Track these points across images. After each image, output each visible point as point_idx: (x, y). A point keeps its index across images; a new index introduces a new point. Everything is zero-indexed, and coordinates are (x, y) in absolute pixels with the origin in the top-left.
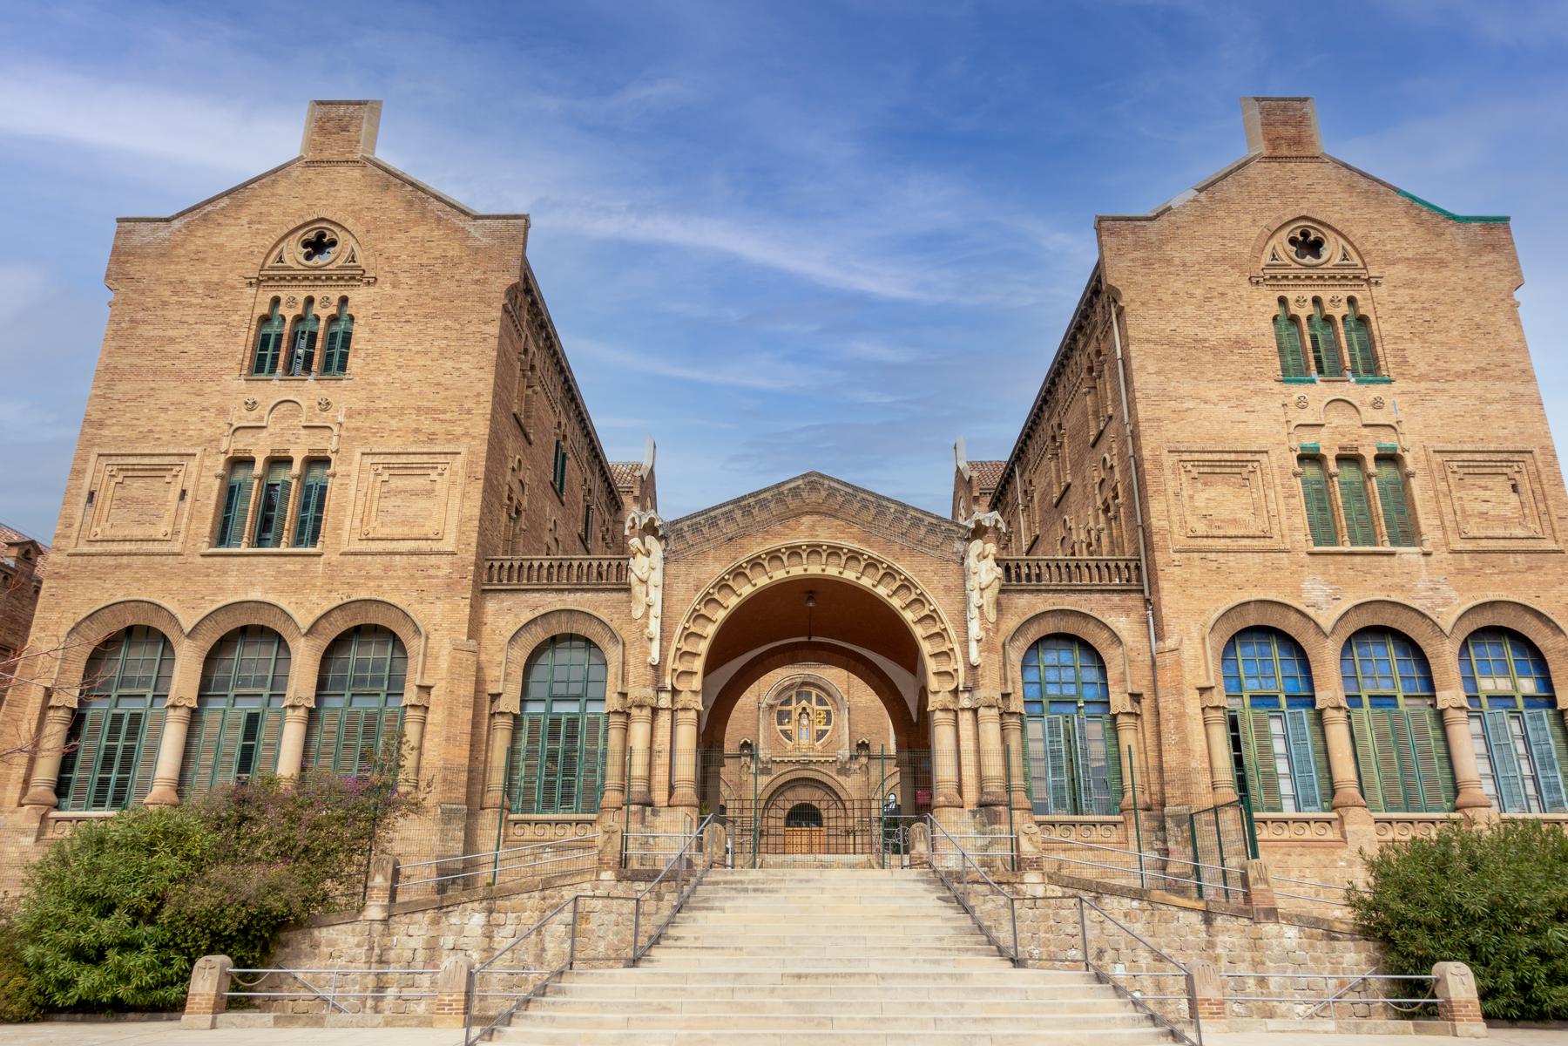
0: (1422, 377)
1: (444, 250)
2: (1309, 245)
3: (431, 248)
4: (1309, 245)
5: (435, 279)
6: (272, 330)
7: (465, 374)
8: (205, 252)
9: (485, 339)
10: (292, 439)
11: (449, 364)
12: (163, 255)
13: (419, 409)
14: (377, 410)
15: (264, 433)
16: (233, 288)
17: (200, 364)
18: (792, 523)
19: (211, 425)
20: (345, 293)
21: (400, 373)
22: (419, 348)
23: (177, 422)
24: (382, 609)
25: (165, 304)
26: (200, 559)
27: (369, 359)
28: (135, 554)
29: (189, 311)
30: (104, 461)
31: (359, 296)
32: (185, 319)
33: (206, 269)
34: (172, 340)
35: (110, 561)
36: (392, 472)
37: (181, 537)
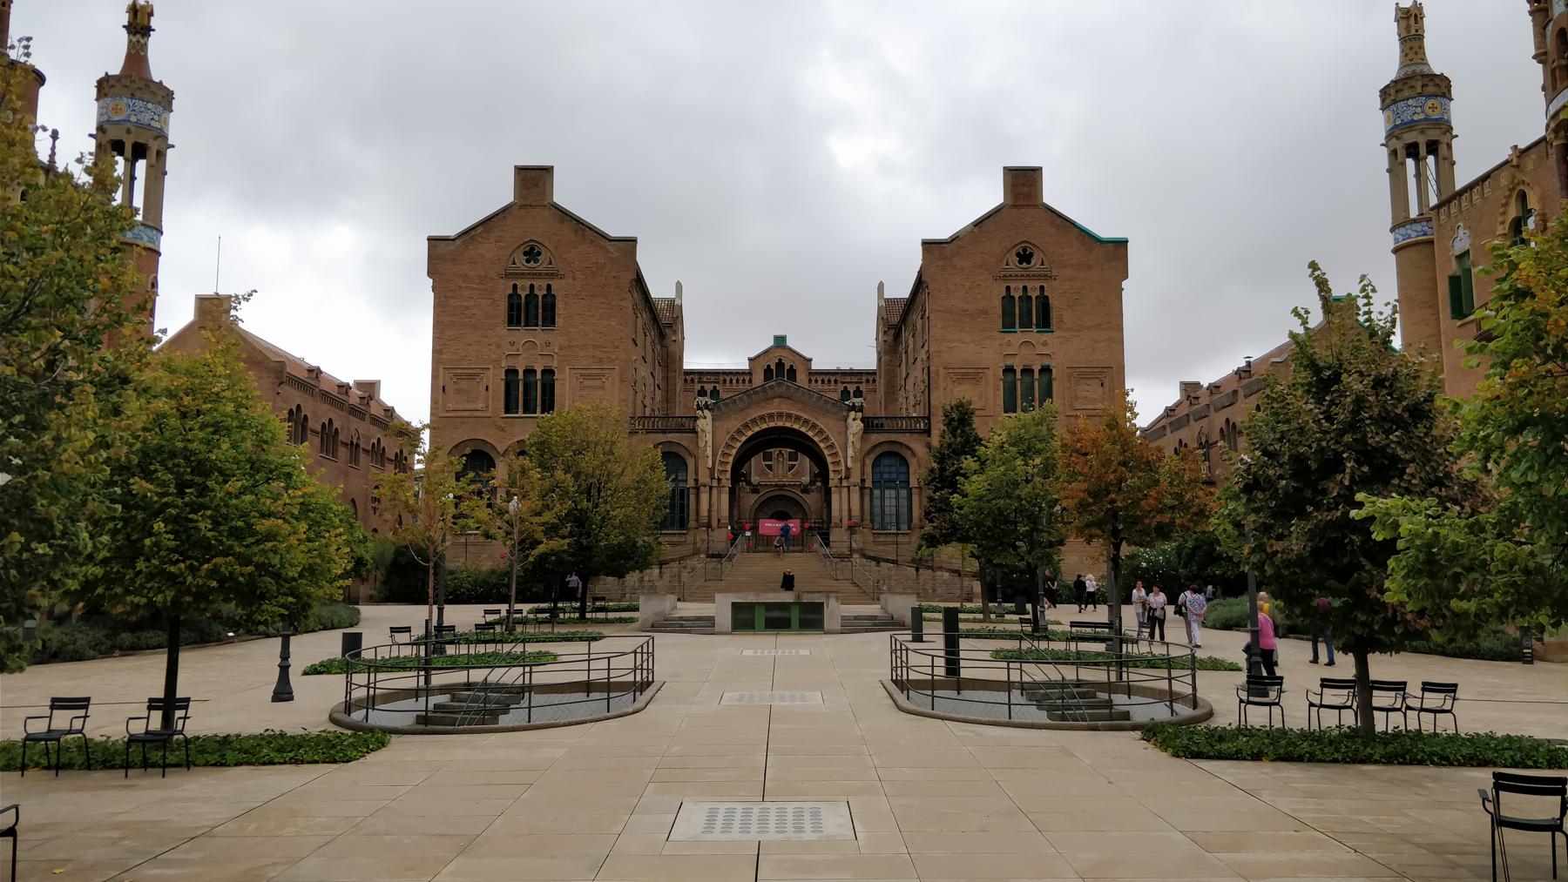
0: (1069, 329)
2: (1025, 257)
4: (1025, 257)
6: (515, 301)
11: (606, 322)
34: (467, 307)
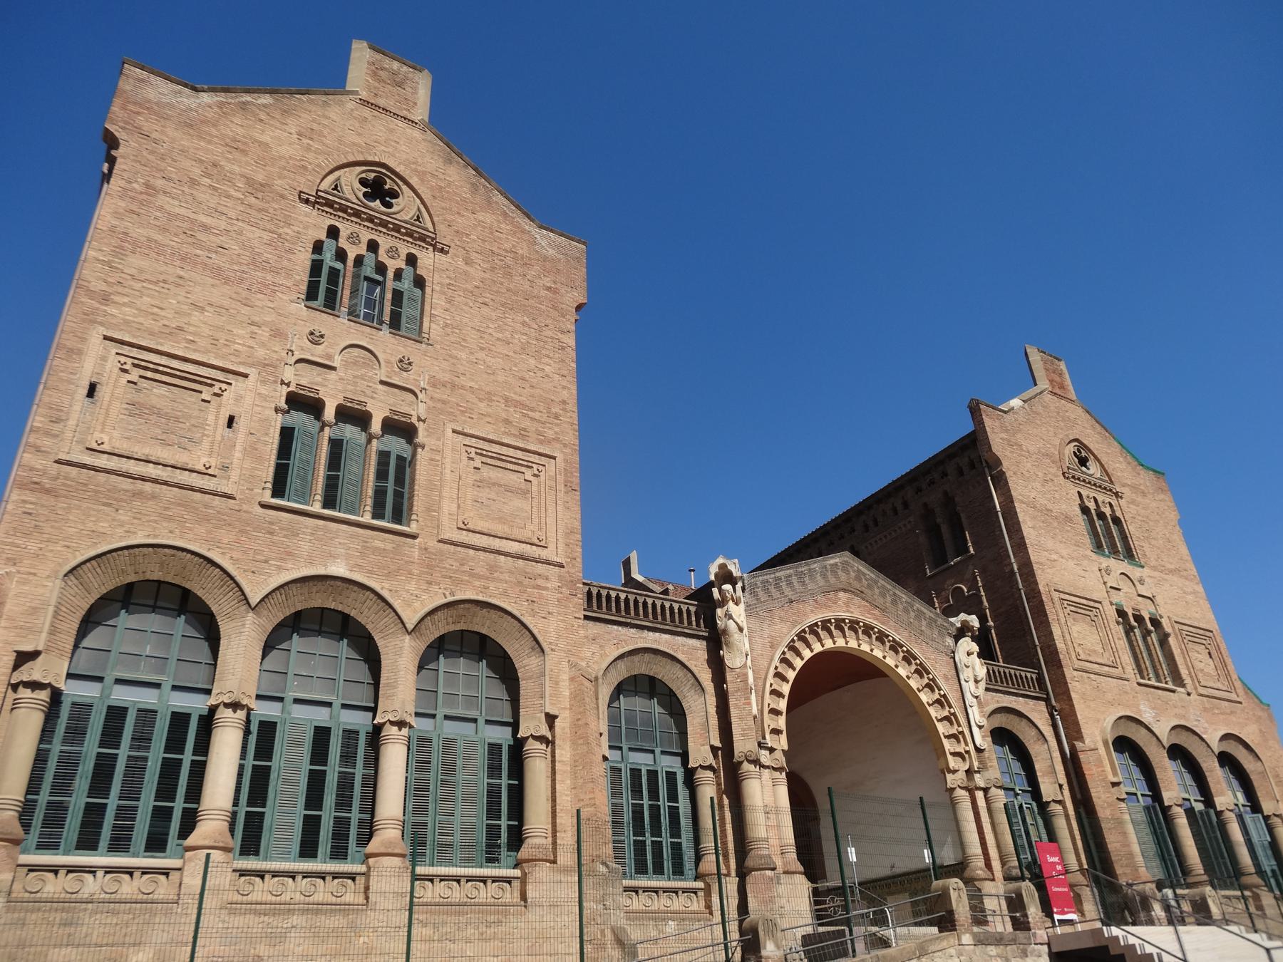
1: (514, 246)
3: (500, 238)
5: (508, 275)
7: (547, 376)
8: (245, 143)
9: (563, 348)
10: (368, 392)
11: (532, 362)
12: (190, 126)
13: (507, 399)
14: (463, 387)
15: (332, 375)
16: (282, 196)
17: (244, 268)
18: (831, 595)
19: (263, 345)
20: (413, 251)
21: (481, 355)
22: (500, 336)
23: (221, 328)
24: (494, 614)
25: (193, 183)
26: (261, 510)
27: (449, 330)
28: (165, 483)
29: (230, 203)
30: (114, 348)
31: (427, 259)
32: (221, 209)
33: (247, 163)
34: (205, 228)
35: (125, 484)
36: (485, 459)
37: (234, 475)
